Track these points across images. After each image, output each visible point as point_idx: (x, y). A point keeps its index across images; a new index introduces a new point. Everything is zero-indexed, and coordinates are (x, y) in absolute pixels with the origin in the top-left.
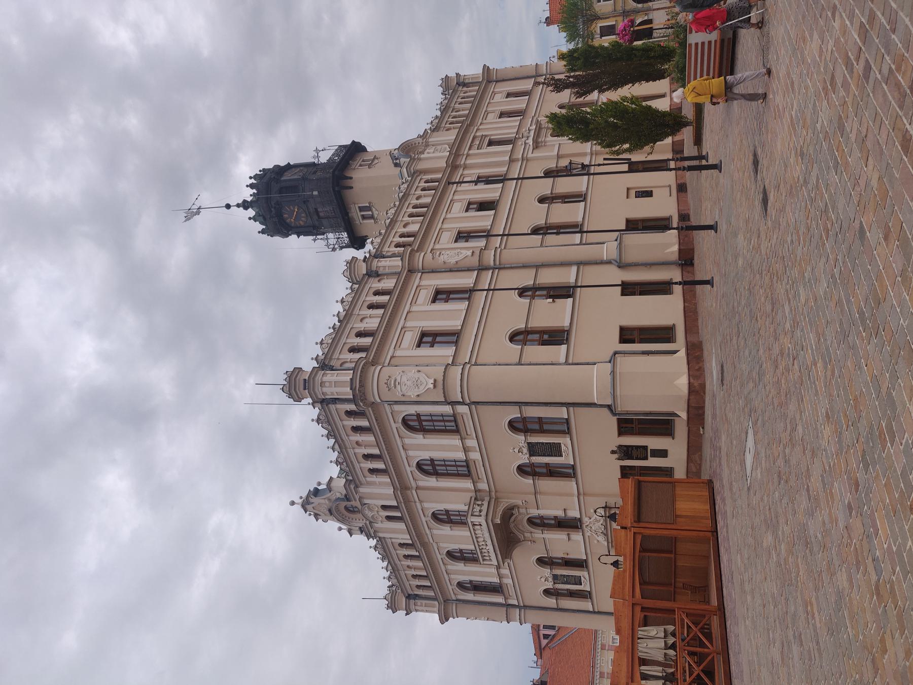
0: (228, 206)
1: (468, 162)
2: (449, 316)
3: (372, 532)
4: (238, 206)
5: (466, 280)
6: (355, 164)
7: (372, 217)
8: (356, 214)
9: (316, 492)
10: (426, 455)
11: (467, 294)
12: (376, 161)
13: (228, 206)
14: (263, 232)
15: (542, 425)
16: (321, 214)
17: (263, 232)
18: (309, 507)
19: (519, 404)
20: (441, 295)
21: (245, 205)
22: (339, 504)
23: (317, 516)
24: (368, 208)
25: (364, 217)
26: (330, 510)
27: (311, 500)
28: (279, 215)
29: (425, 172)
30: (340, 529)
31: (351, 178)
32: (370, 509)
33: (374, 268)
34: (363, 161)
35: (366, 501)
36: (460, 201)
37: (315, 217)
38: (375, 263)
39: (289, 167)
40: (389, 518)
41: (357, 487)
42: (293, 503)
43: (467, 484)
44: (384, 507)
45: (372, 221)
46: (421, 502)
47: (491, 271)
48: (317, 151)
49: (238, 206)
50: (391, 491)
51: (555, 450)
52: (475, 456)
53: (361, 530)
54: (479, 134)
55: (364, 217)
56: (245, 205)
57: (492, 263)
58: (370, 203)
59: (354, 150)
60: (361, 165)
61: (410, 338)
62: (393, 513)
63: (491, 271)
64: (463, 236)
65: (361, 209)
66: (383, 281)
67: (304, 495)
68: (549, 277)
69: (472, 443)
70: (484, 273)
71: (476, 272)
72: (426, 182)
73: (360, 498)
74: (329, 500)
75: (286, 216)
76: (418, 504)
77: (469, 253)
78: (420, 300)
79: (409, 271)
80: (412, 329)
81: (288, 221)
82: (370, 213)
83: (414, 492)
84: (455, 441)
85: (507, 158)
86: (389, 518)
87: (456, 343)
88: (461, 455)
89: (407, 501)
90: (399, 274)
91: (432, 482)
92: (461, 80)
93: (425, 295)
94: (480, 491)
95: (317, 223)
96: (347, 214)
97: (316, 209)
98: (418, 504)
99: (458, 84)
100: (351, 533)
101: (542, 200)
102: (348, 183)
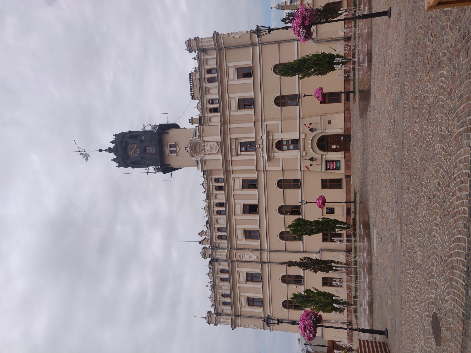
0: (100, 151)
4: (106, 150)
8: (167, 149)
13: (100, 151)
17: (114, 160)
21: (110, 150)
24: (175, 146)
45: (175, 154)
49: (106, 150)
55: (171, 152)
56: (110, 150)
58: (176, 143)
65: (171, 146)
75: (129, 150)
81: (129, 154)
82: (175, 149)
96: (162, 149)
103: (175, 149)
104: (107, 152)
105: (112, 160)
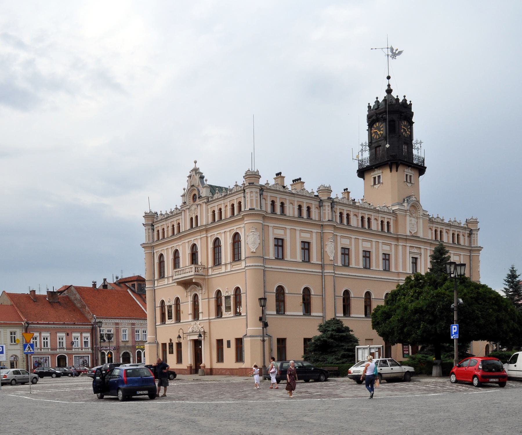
0: (389, 78)
1: (400, 248)
2: (293, 252)
3: (184, 209)
4: (389, 86)
5: (315, 258)
6: (409, 171)
7: (375, 184)
8: (377, 173)
9: (202, 178)
10: (222, 244)
11: (307, 259)
12: (409, 185)
13: (389, 78)
14: (369, 107)
15: (238, 303)
16: (378, 148)
18: (194, 173)
19: (246, 293)
20: (306, 246)
21: (389, 91)
22: (198, 190)
23: (190, 177)
24: (379, 183)
25: (375, 178)
26: (193, 186)
27: (197, 175)
28: (377, 120)
29: (396, 221)
30: (184, 189)
31: (397, 171)
32: (195, 209)
33: (324, 204)
34: (410, 176)
35: (199, 207)
36: (372, 245)
37: (376, 145)
38: (327, 205)
39: (411, 123)
40: (192, 219)
41: (206, 203)
42: (195, 162)
43: (210, 264)
44: (197, 217)
46: (201, 238)
47: (321, 271)
48: (421, 142)
49: (389, 86)
50: (204, 223)
51: (228, 308)
52: (223, 269)
53: (185, 203)
54: (422, 251)
55: (375, 178)
56: (389, 91)
57: (325, 271)
58: (382, 183)
59: (421, 169)
60: (407, 175)
61: (280, 233)
62: (194, 221)
63: (321, 271)
64: (346, 252)
65: (379, 177)
66: (317, 210)
67: (201, 171)
68: (315, 302)
69: (229, 268)
70: (320, 267)
71: (320, 263)
72: (388, 223)
73: (201, 205)
74: (199, 185)
75: (377, 124)
76: (199, 237)
77: (332, 258)
78: (303, 235)
79: (322, 225)
80: (285, 234)
83: (205, 235)
84: (229, 259)
85: (401, 271)
86: (192, 219)
87: (277, 258)
88: (223, 262)
89: (200, 231)
90: (320, 221)
91: (211, 246)
92: (473, 232)
93: (306, 237)
94: (208, 270)
95: (373, 145)
96: (376, 168)
97: (380, 146)
98: (199, 237)
99: (471, 230)
100: (183, 196)
101: (368, 294)
102: (394, 170)
103: (377, 183)
104: (386, 88)
105: (369, 104)
